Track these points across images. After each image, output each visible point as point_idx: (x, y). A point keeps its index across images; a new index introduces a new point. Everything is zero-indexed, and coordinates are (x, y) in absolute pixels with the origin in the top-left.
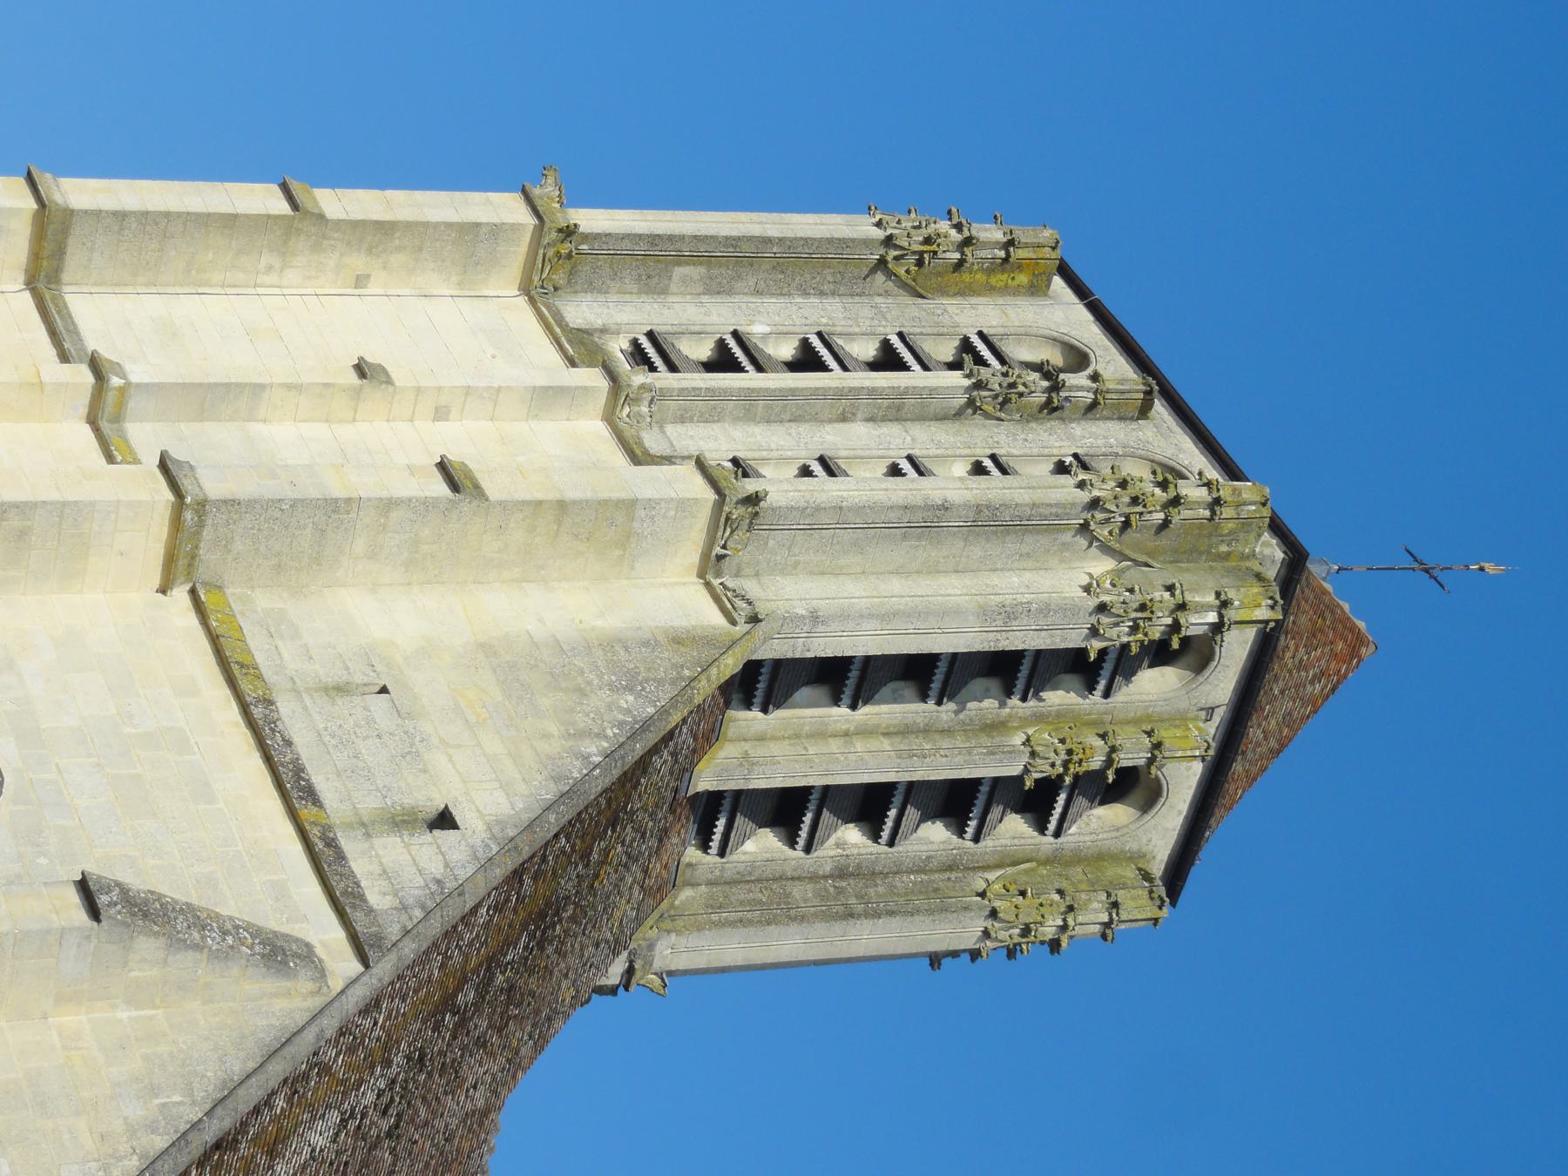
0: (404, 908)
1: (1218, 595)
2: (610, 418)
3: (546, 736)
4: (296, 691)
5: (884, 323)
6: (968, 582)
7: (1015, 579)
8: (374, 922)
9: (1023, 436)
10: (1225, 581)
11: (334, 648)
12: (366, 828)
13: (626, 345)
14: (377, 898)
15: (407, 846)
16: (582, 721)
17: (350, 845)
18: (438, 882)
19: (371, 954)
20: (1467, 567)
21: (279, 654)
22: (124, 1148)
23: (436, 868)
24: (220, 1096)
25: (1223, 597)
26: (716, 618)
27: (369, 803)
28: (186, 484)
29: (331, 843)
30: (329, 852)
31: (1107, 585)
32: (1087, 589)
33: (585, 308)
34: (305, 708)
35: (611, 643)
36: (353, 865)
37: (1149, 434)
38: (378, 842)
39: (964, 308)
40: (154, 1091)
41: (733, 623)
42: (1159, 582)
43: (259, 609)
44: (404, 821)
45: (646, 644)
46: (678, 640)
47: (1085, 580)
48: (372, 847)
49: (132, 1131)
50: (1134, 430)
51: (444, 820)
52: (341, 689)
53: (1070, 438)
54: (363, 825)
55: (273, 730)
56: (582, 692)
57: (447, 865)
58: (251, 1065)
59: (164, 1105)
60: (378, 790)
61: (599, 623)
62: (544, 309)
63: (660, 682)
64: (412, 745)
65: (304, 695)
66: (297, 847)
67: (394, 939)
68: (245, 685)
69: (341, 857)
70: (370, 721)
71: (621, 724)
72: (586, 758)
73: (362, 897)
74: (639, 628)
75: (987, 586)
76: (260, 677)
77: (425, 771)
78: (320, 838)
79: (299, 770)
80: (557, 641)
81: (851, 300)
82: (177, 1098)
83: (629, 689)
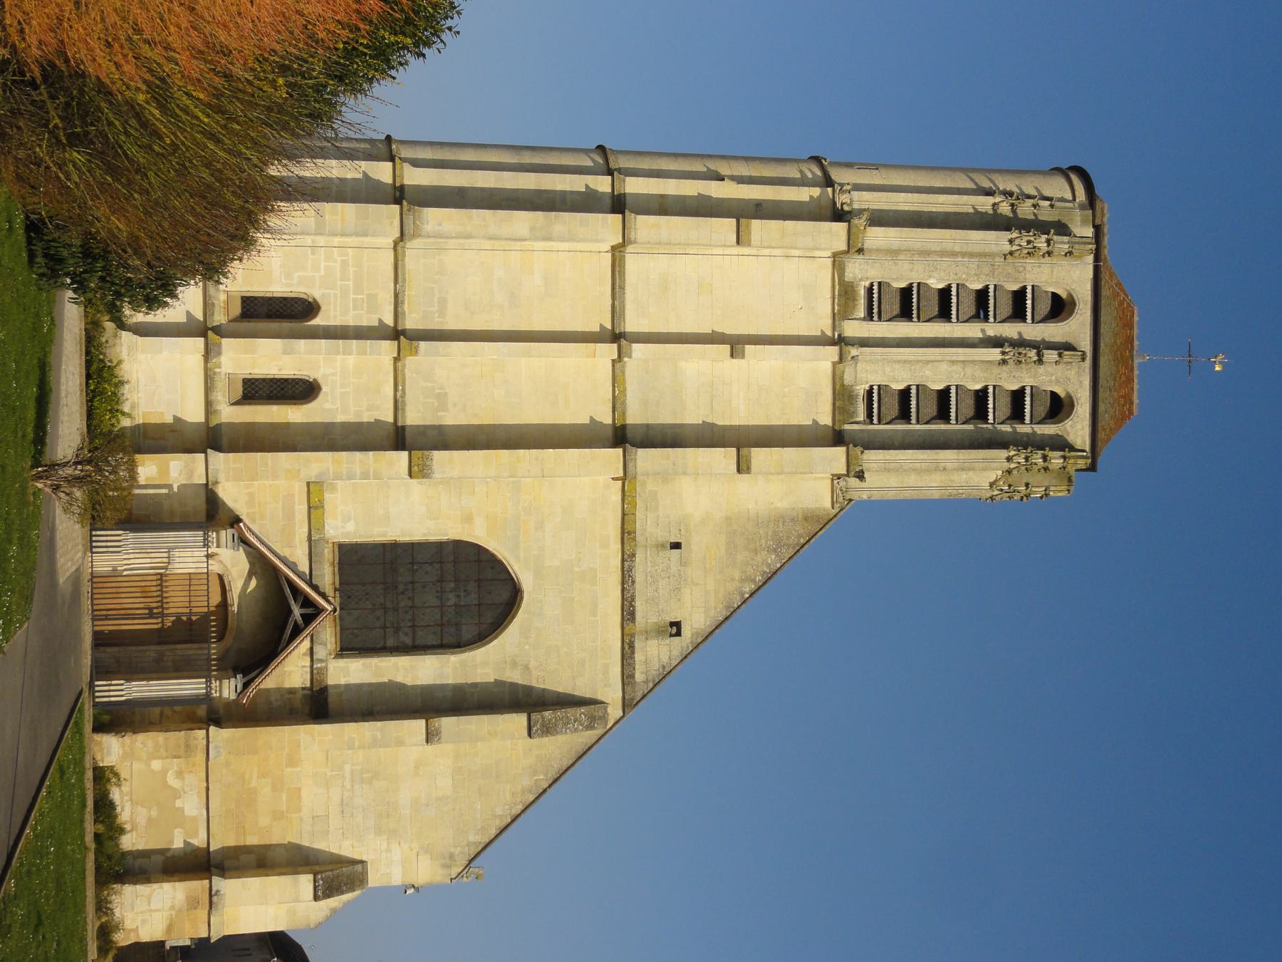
0: (646, 682)
1: (1046, 490)
2: (834, 364)
3: (733, 579)
4: (646, 547)
5: (991, 279)
6: (943, 477)
7: (964, 476)
8: (634, 692)
9: (1014, 374)
10: (1054, 482)
11: (669, 518)
12: (647, 634)
13: (867, 284)
14: (639, 677)
15: (659, 645)
16: (750, 570)
17: (637, 645)
18: (664, 667)
19: (626, 710)
20: (1209, 359)
21: (646, 522)
22: (519, 800)
23: (665, 659)
24: (556, 777)
25: (1047, 492)
26: (828, 505)
27: (653, 619)
28: (630, 465)
29: (632, 646)
30: (629, 651)
31: (1001, 483)
32: (991, 485)
33: (857, 264)
34: (646, 558)
35: (781, 518)
36: (636, 655)
37: (1073, 373)
38: (649, 642)
39: (1035, 266)
40: (535, 773)
41: (833, 508)
42: (1025, 481)
43: (647, 491)
44: (663, 631)
45: (792, 520)
46: (808, 517)
47: (992, 480)
48: (646, 647)
49: (523, 792)
50: (1067, 369)
51: (677, 625)
52: (663, 546)
53: (1035, 376)
54: (647, 632)
55: (629, 576)
56: (755, 551)
57: (669, 658)
58: (571, 762)
59: (537, 780)
60: (658, 612)
61: (779, 505)
62: (836, 274)
63: (788, 546)
64: (680, 582)
65: (648, 549)
66: (619, 644)
67: (638, 699)
68: (627, 547)
69: (633, 653)
70: (669, 567)
71: (765, 572)
72: (742, 594)
73: (632, 676)
74: (794, 509)
75: (951, 481)
76: (634, 539)
77: (679, 600)
78: (628, 644)
79: (633, 599)
80: (758, 513)
81: (984, 260)
82: (541, 777)
83: (775, 550)
